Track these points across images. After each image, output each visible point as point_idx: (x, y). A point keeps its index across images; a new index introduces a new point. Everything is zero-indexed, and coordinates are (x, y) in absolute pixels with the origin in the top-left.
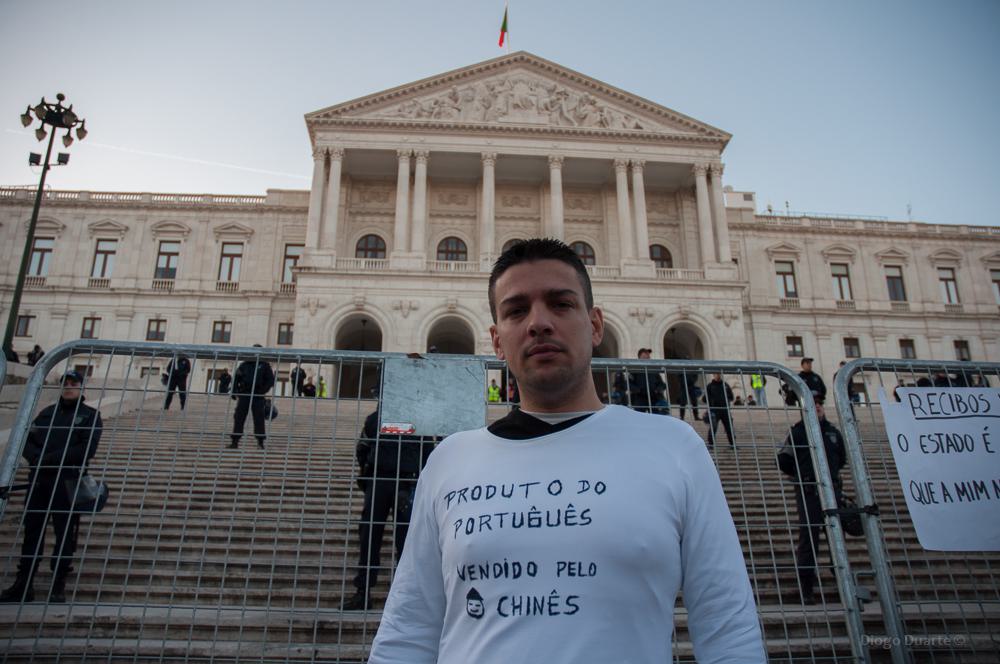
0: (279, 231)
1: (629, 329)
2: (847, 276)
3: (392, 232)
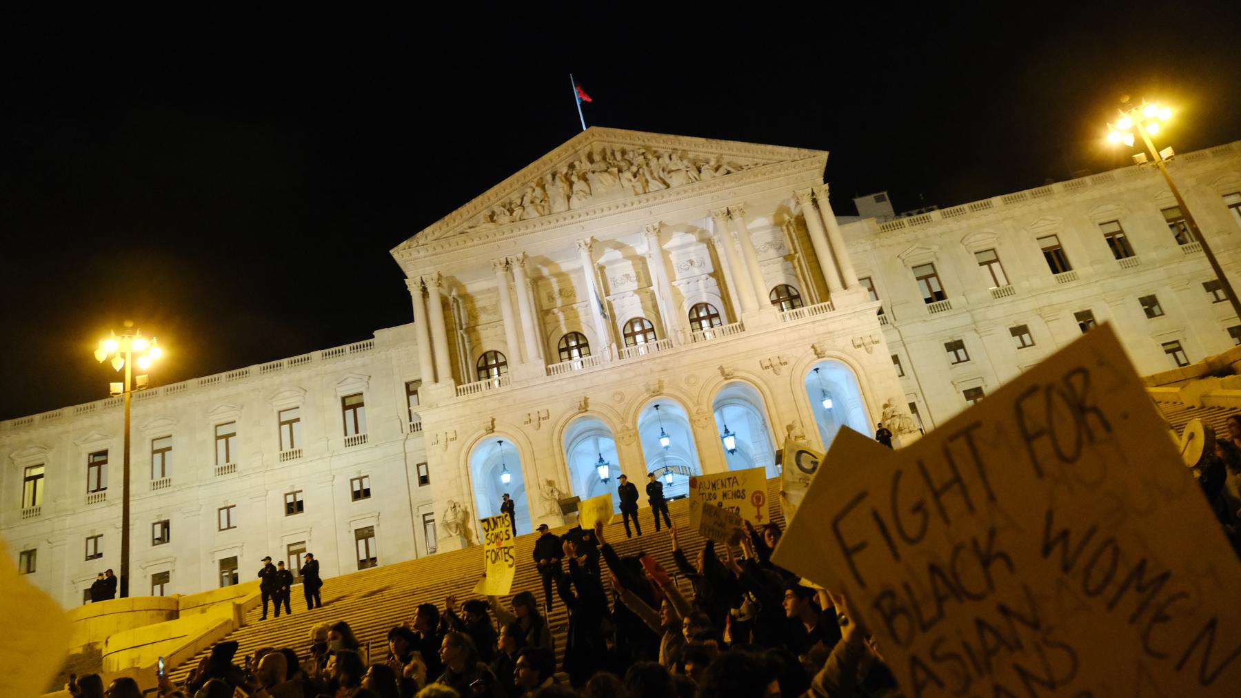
1: (766, 383)
2: (997, 260)
3: (505, 343)
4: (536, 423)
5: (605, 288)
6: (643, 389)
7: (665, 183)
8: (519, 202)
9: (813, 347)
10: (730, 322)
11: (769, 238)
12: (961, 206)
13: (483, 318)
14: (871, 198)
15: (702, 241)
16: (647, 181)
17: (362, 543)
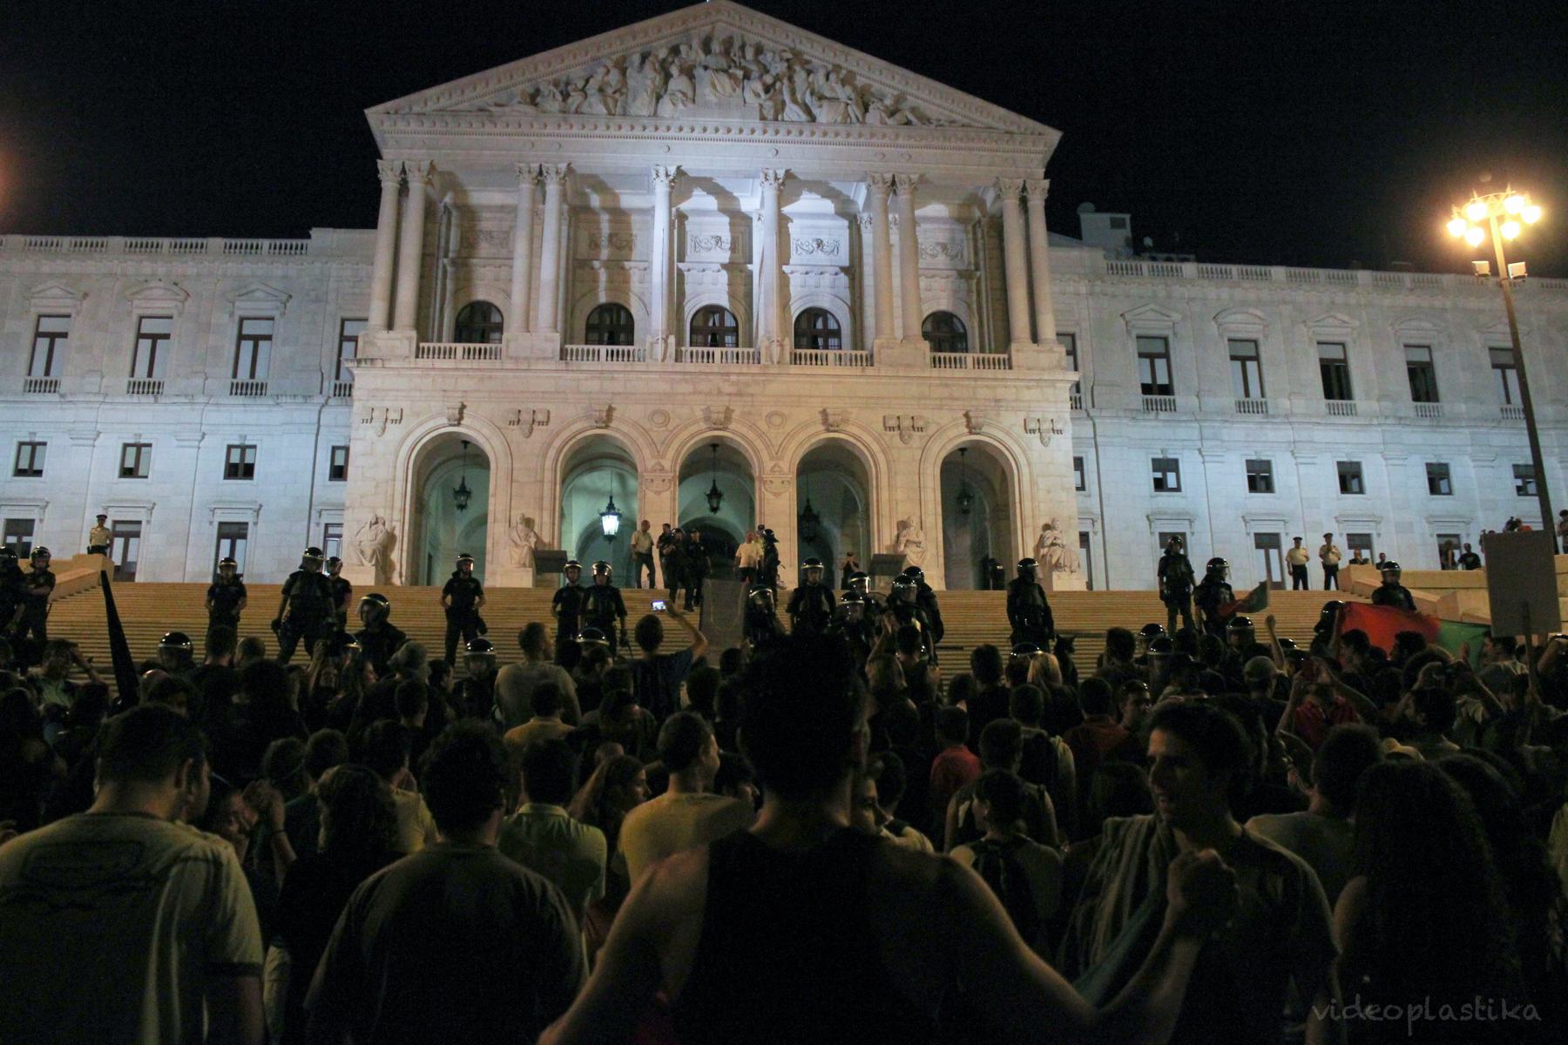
0: (332, 296)
1: (884, 452)
2: (1256, 358)
3: (508, 295)
4: (526, 427)
5: (679, 248)
6: (699, 414)
7: (808, 111)
8: (580, 84)
9: (966, 415)
10: (855, 347)
12: (1229, 267)
13: (485, 249)
14: (1105, 218)
16: (784, 103)
17: (226, 543)
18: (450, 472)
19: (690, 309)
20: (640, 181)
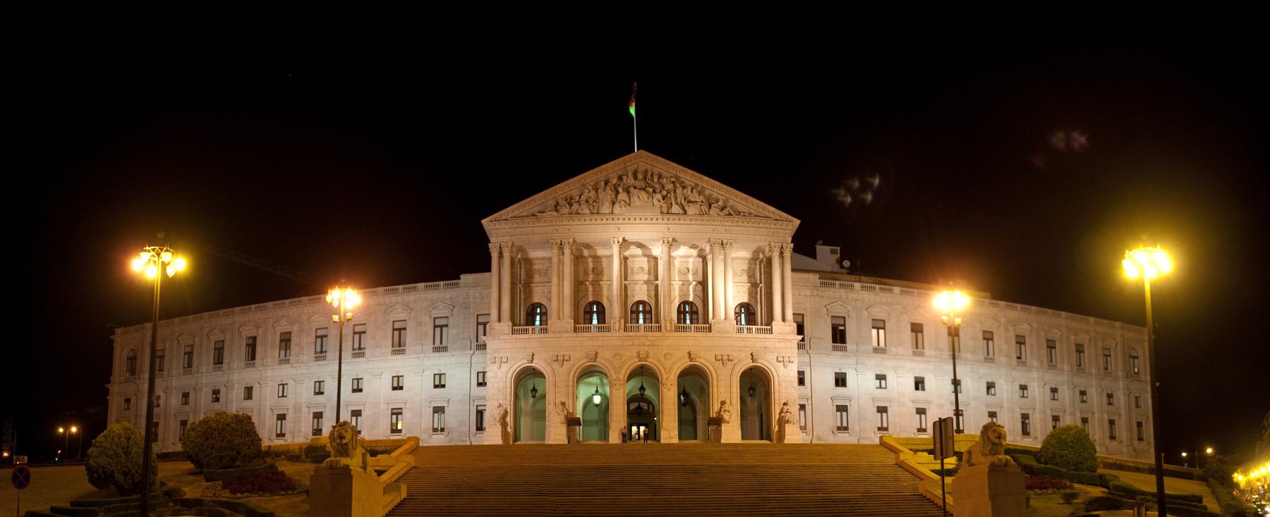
3: (549, 299)
11: (745, 267)
15: (699, 256)
18: (527, 379)
19: (630, 304)
20: (607, 244)
